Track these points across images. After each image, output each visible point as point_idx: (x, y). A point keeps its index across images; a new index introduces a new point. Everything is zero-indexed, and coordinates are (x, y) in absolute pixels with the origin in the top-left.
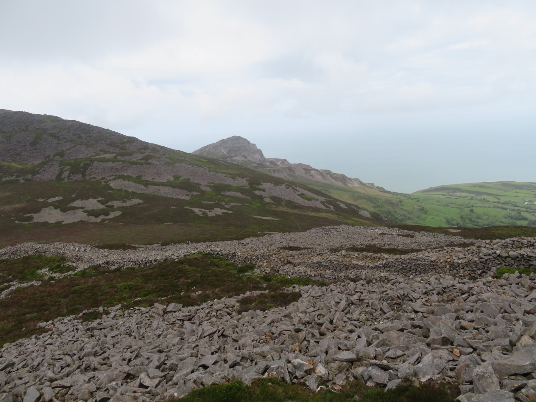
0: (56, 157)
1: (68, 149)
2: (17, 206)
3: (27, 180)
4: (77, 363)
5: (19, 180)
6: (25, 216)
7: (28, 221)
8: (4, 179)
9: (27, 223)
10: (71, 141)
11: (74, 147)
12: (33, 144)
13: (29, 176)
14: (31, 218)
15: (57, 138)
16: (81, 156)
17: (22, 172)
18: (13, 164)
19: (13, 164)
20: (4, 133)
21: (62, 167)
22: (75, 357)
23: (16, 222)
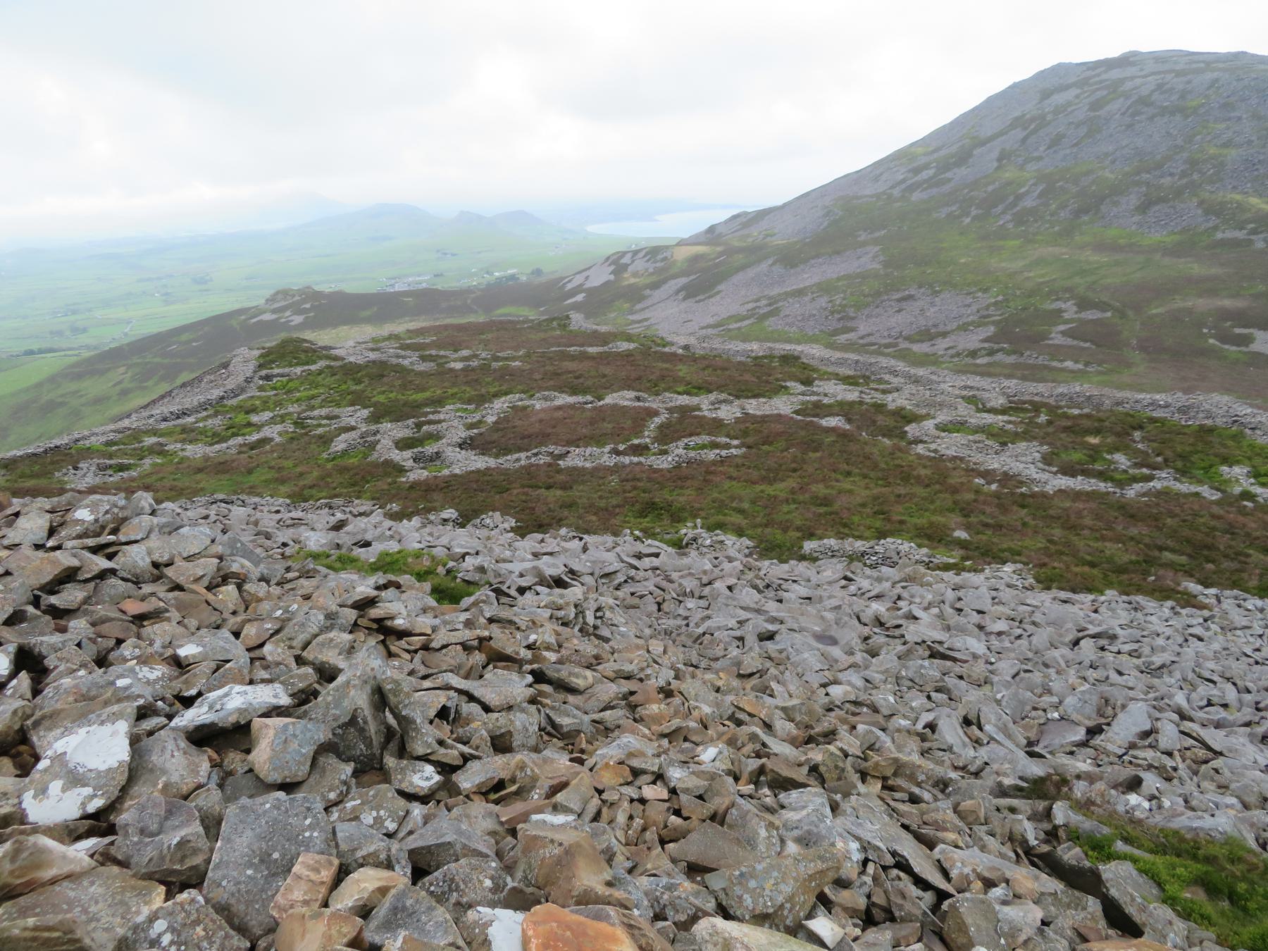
2: (1227, 303)
4: (1248, 714)
5: (1250, 242)
6: (1237, 331)
7: (1238, 345)
8: (1219, 235)
9: (1234, 348)
14: (1246, 340)
18: (1254, 201)
19: (1254, 201)
22: (1248, 698)
23: (1211, 341)
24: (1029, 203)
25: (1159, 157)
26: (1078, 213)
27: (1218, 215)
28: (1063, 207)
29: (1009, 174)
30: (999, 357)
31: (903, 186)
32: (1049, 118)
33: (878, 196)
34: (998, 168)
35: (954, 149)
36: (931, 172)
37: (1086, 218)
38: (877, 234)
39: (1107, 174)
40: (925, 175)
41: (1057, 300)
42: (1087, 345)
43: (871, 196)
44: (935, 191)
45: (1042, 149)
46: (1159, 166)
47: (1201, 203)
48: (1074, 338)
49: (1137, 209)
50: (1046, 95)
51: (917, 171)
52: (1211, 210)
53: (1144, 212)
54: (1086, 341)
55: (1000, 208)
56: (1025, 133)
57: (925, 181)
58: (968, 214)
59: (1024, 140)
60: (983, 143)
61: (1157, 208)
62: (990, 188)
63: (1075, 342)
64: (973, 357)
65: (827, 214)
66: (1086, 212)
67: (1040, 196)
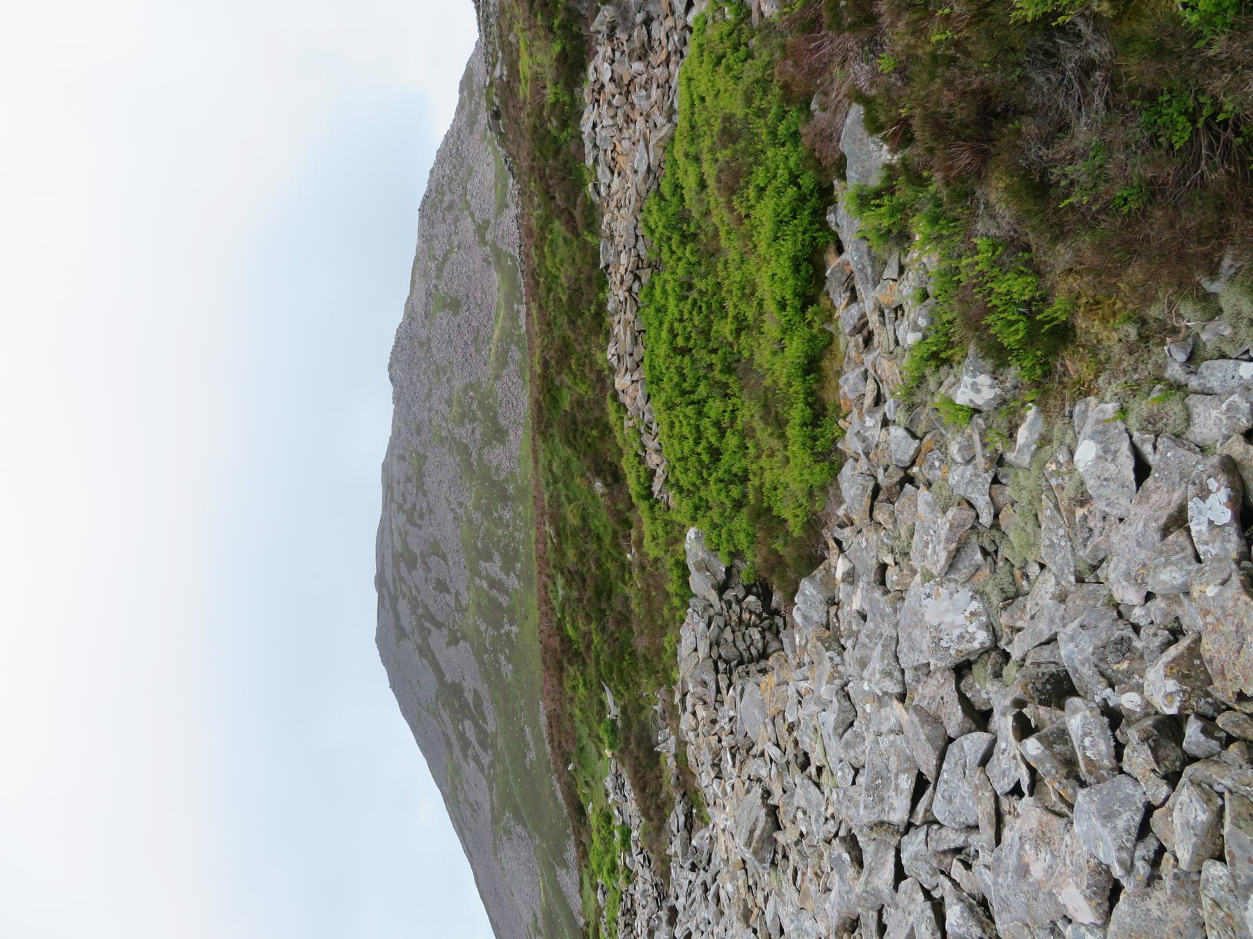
0: (488, 237)
1: (472, 216)
10: (457, 219)
11: (468, 206)
12: (454, 305)
15: (448, 252)
16: (491, 176)
18: (497, 333)
20: (430, 390)
21: (508, 197)
24: (494, 568)
25: (458, 458)
26: (505, 498)
27: (507, 351)
28: (499, 522)
29: (472, 619)
31: (481, 753)
32: (420, 611)
33: (490, 781)
34: (464, 637)
35: (446, 715)
36: (467, 723)
37: (511, 488)
38: (529, 737)
39: (470, 504)
40: (471, 733)
43: (491, 790)
44: (488, 706)
45: (448, 598)
46: (464, 450)
49: (502, 442)
50: (402, 633)
51: (466, 744)
53: (506, 432)
55: (503, 600)
56: (433, 629)
57: (477, 725)
58: (508, 634)
59: (439, 625)
60: (440, 675)
61: (503, 422)
65: (508, 832)
66: (505, 490)
67: (489, 558)
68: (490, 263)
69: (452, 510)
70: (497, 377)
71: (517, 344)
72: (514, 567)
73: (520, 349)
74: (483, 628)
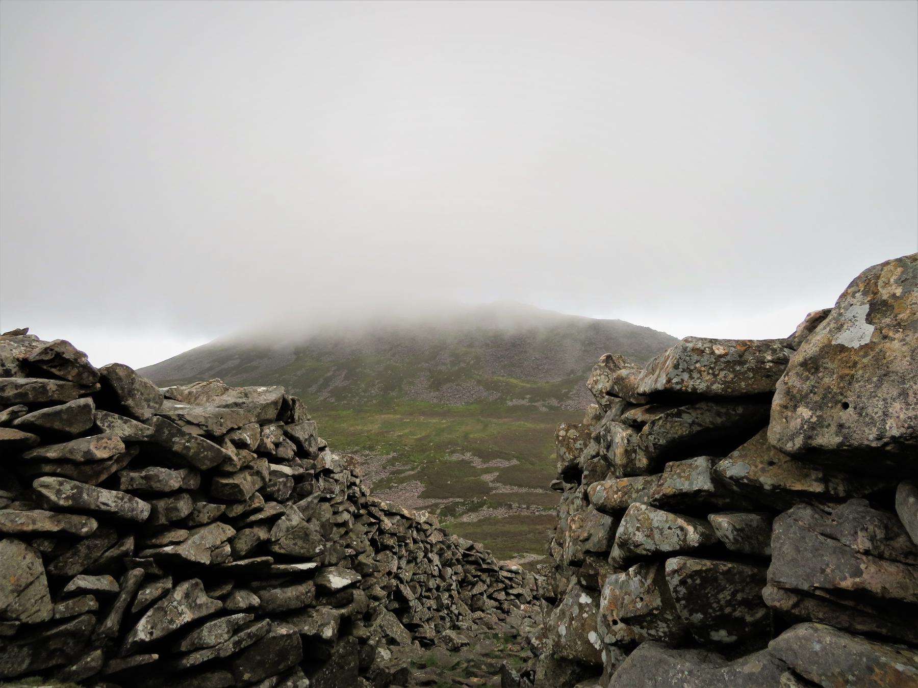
3: (551, 408)
8: (510, 403)
13: (554, 402)
17: (538, 394)
24: (338, 383)
30: (485, 512)
37: (394, 394)
41: (453, 452)
42: (540, 491)
47: (479, 382)
48: (520, 486)
49: (430, 387)
52: (491, 386)
53: (438, 390)
54: (535, 488)
55: (314, 388)
61: (445, 387)
62: (299, 373)
63: (524, 490)
64: (453, 515)
68: (569, 375)
69: (391, 349)
70: (479, 382)
71: (501, 398)
72: (332, 396)
73: (496, 400)
74: (299, 373)
